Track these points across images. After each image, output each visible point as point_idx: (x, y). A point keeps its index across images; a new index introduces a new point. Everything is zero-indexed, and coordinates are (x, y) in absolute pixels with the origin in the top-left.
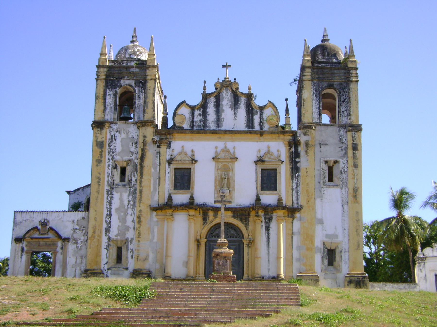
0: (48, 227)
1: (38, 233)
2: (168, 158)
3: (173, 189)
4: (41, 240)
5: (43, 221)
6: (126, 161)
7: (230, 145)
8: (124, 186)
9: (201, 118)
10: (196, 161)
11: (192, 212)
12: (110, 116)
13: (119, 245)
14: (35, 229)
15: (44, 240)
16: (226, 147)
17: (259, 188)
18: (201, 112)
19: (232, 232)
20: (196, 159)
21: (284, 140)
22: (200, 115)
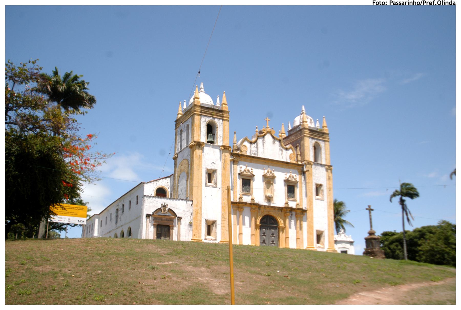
0: (167, 209)
1: (160, 211)
2: (239, 172)
3: (241, 191)
4: (164, 217)
5: (163, 204)
6: (213, 170)
8: (213, 186)
9: (255, 149)
10: (254, 175)
11: (254, 207)
12: (203, 138)
13: (209, 224)
14: (160, 209)
15: (166, 217)
17: (287, 196)
18: (255, 145)
19: (273, 221)
20: (254, 174)
21: (298, 169)
22: (255, 147)
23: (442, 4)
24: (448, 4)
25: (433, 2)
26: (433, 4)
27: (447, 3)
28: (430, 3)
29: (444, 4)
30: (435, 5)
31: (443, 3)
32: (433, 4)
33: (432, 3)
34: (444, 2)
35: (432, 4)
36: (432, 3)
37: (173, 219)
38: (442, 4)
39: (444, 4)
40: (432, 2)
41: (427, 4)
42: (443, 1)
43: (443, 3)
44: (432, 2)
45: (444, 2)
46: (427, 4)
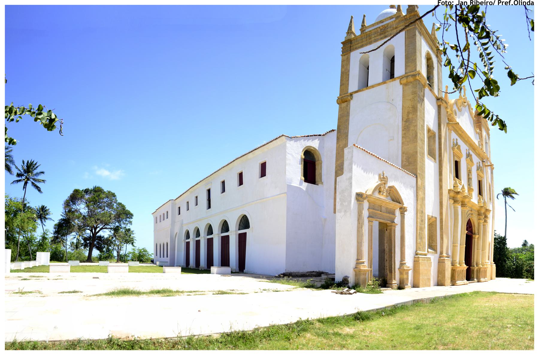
41: (502, 5)
46: (502, 5)
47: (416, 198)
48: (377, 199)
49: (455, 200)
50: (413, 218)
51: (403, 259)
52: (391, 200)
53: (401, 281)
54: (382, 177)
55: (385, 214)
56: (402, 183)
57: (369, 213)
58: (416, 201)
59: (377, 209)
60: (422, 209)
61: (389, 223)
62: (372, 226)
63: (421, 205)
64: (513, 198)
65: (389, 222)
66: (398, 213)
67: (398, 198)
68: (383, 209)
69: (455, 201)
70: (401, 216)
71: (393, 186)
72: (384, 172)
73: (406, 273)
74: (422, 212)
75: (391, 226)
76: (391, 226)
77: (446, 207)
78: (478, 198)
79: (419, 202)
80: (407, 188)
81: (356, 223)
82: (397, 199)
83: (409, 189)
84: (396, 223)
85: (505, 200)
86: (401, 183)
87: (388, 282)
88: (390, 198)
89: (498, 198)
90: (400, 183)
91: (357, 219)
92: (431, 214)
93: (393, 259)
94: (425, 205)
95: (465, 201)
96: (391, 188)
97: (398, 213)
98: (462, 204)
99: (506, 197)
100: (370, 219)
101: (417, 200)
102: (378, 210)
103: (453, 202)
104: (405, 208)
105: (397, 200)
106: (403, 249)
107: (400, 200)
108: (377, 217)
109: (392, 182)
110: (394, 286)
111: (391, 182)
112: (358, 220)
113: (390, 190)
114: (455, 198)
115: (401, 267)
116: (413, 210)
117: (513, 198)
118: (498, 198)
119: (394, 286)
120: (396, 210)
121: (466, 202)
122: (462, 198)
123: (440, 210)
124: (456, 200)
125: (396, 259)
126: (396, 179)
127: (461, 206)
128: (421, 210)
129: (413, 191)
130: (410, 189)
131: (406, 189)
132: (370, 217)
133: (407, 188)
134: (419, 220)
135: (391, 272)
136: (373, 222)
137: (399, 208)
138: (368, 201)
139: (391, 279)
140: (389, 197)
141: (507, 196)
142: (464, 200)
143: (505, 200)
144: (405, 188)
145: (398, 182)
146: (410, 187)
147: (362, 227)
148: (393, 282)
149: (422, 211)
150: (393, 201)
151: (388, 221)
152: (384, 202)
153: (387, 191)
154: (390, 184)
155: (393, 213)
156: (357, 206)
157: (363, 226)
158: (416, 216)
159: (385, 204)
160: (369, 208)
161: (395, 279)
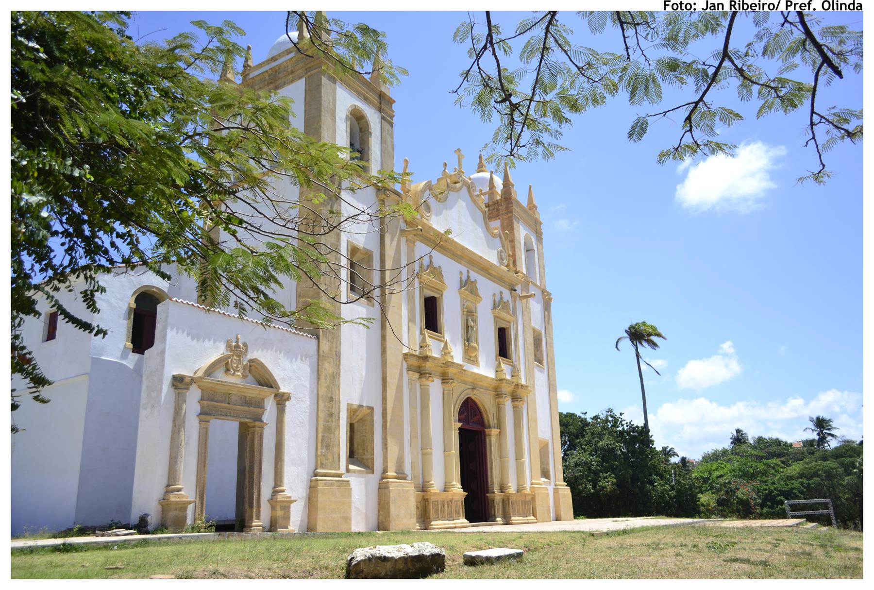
7: (474, 276)
16: (468, 277)
23: (833, 9)
24: (846, 9)
25: (809, 4)
26: (809, 9)
27: (843, 6)
28: (800, 7)
29: (837, 9)
30: (812, 9)
31: (835, 6)
32: (809, 9)
33: (806, 6)
34: (837, 4)
35: (807, 8)
36: (806, 6)
37: (263, 399)
38: (833, 9)
39: (837, 9)
40: (806, 3)
42: (835, 2)
43: (835, 6)
44: (806, 3)
45: (837, 4)
47: (315, 376)
48: (217, 384)
49: (422, 372)
50: (307, 411)
51: (279, 483)
52: (256, 383)
53: (273, 522)
54: (234, 344)
55: (239, 407)
56: (280, 353)
57: (202, 408)
58: (316, 381)
59: (221, 399)
60: (332, 394)
61: (250, 423)
62: (207, 429)
63: (328, 387)
64: (654, 345)
65: (247, 420)
66: (270, 405)
67: (267, 379)
68: (234, 398)
69: (422, 373)
70: (278, 409)
71: (256, 359)
72: (239, 336)
73: (281, 507)
74: (332, 400)
75: (254, 427)
76: (254, 427)
77: (395, 388)
78: (497, 363)
79: (322, 380)
80: (294, 359)
81: (169, 425)
82: (266, 380)
83: (299, 360)
84: (265, 421)
85: (637, 350)
86: (278, 352)
87: (246, 524)
88: (253, 379)
89: (617, 349)
90: (276, 351)
91: (171, 418)
92: (356, 402)
93: (255, 486)
94: (339, 386)
95: (448, 373)
96: (253, 362)
97: (270, 405)
98: (444, 378)
99: (639, 345)
100: (202, 417)
101: (319, 379)
102: (223, 402)
103: (417, 375)
104: (284, 394)
105: (266, 381)
106: (279, 466)
107: (271, 381)
108: (219, 413)
109: (258, 351)
110: (254, 529)
111: (255, 352)
112: (174, 420)
113: (250, 366)
114: (421, 369)
115: (274, 497)
116: (308, 398)
117: (654, 345)
118: (617, 349)
119: (256, 531)
120: (266, 400)
121: (450, 375)
122: (441, 367)
123: (383, 392)
124: (424, 372)
125: (262, 483)
126: (266, 345)
127: (442, 383)
128: (329, 395)
129: (309, 363)
130: (302, 360)
131: (291, 362)
132: (203, 413)
133: (294, 359)
134: (321, 415)
135: (251, 506)
136: (209, 422)
137: (273, 395)
138: (200, 387)
139: (251, 519)
140: (250, 377)
141: (641, 344)
142: (447, 371)
143: (637, 350)
144: (289, 360)
145: (272, 350)
146: (302, 356)
147: (179, 432)
148: (253, 524)
149: (332, 398)
150: (261, 385)
151: (247, 418)
152: (234, 387)
153: (244, 368)
154: (251, 355)
155: (259, 404)
156: (174, 398)
157: (183, 430)
158: (315, 407)
159: (238, 391)
160: (201, 400)
161: (258, 518)
